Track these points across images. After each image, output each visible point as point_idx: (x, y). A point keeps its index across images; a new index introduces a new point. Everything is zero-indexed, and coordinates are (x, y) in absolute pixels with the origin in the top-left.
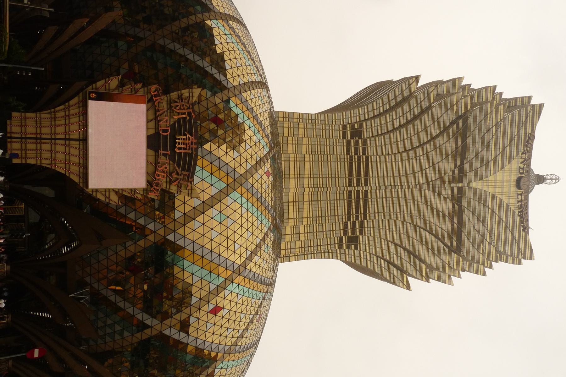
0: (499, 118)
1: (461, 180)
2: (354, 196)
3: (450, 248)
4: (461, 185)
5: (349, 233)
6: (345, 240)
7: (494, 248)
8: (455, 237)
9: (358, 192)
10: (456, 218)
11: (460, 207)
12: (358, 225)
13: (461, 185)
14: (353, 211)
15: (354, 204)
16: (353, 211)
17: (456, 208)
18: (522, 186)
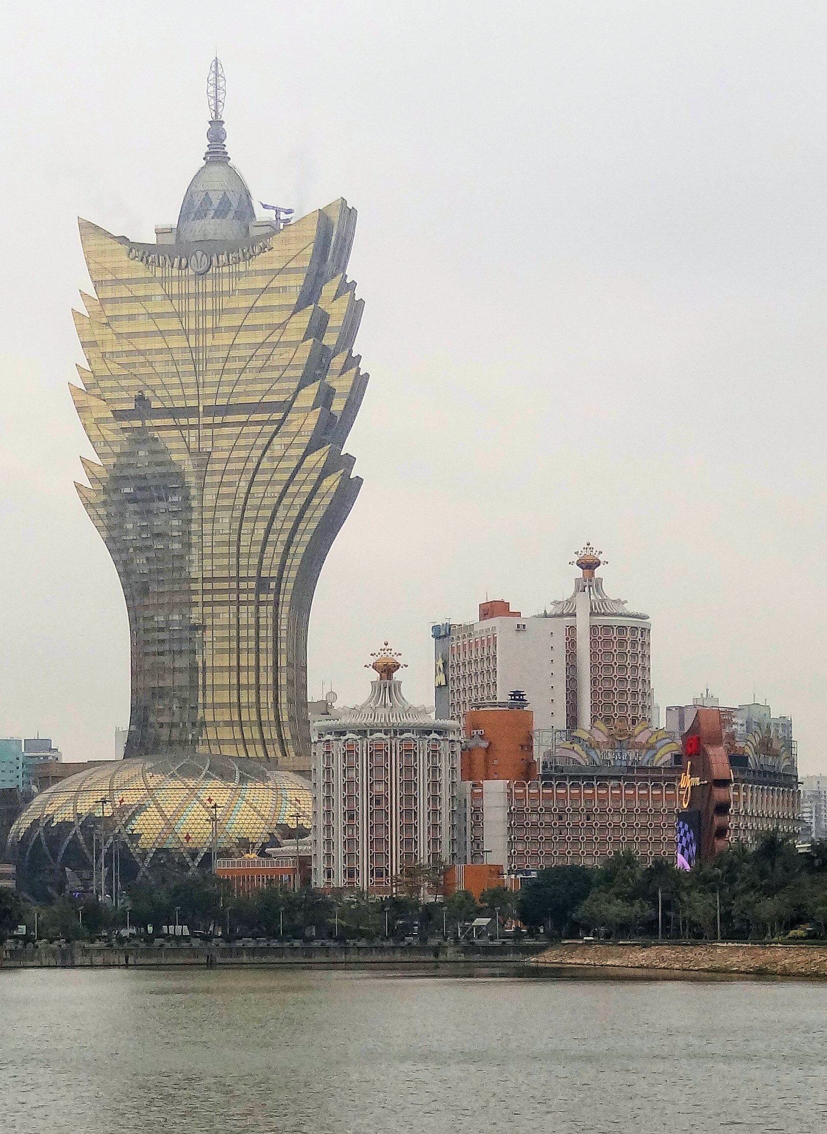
0: (109, 337)
1: (191, 412)
2: (208, 598)
3: (281, 422)
4: (201, 409)
5: (252, 597)
6: (263, 597)
7: (293, 319)
8: (265, 417)
9: (204, 592)
10: (243, 418)
11: (227, 409)
12: (243, 585)
13: (201, 409)
14: (225, 597)
15: (217, 597)
16: (225, 597)
17: (230, 419)
18: (204, 268)
